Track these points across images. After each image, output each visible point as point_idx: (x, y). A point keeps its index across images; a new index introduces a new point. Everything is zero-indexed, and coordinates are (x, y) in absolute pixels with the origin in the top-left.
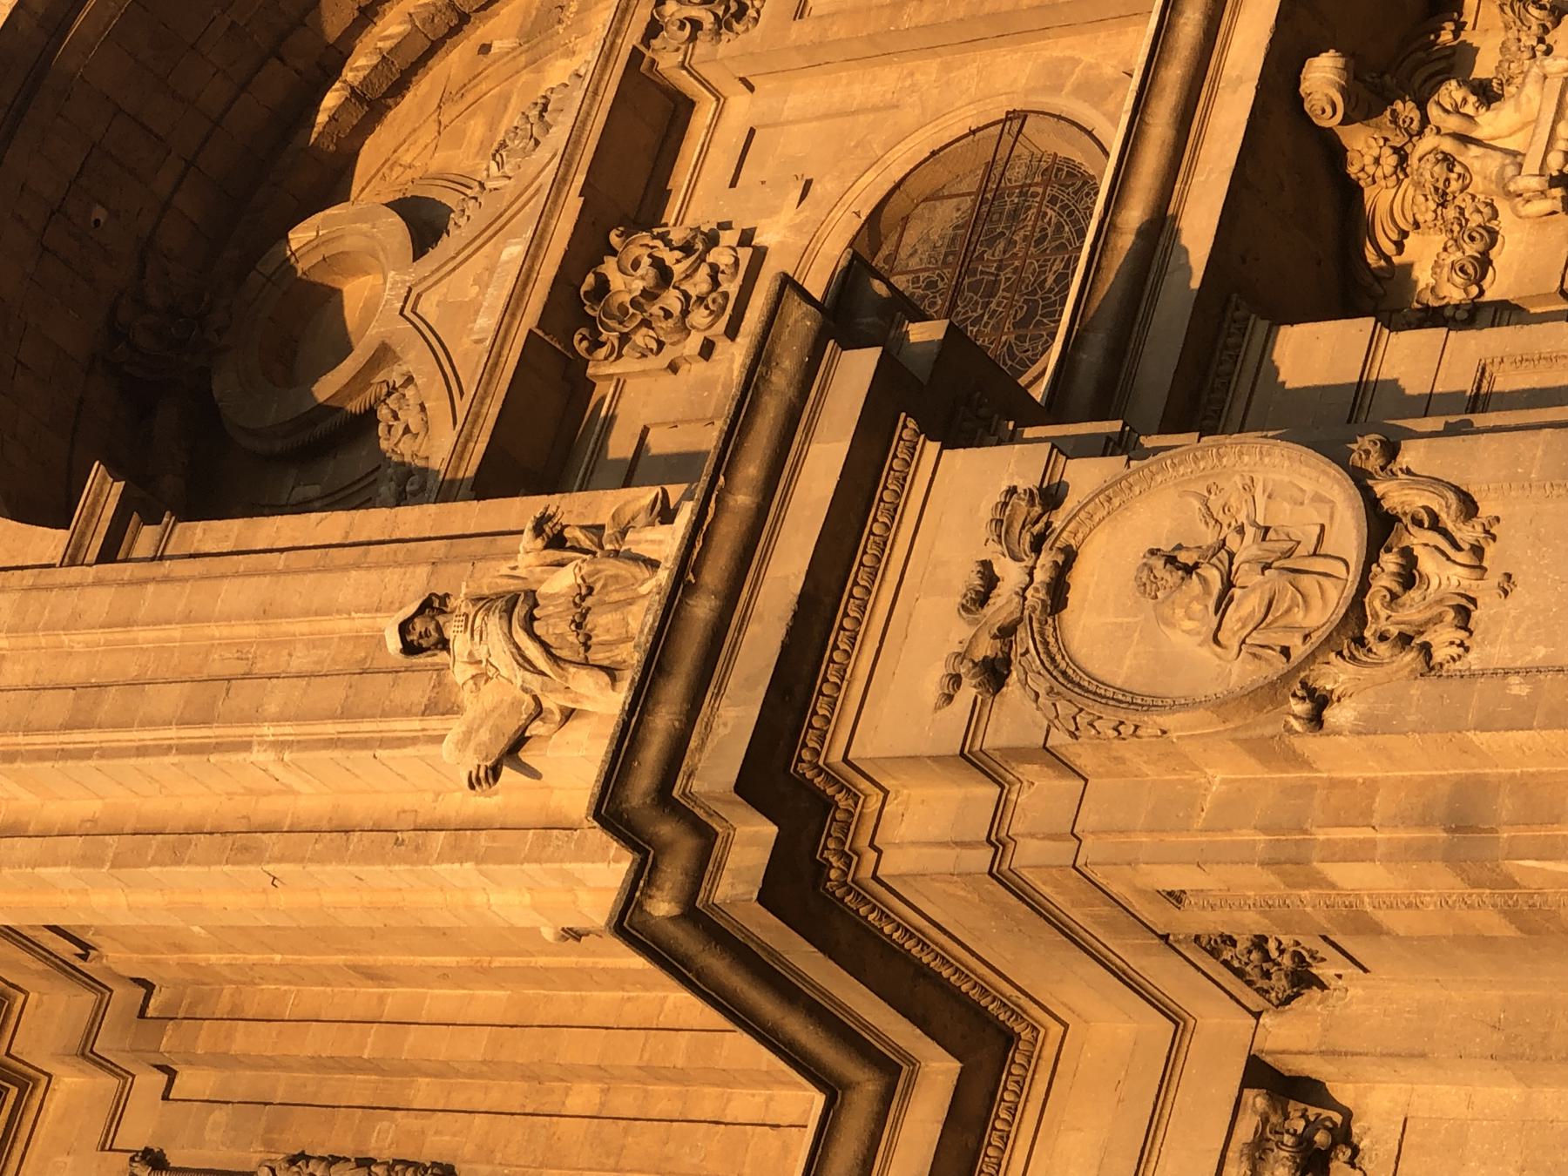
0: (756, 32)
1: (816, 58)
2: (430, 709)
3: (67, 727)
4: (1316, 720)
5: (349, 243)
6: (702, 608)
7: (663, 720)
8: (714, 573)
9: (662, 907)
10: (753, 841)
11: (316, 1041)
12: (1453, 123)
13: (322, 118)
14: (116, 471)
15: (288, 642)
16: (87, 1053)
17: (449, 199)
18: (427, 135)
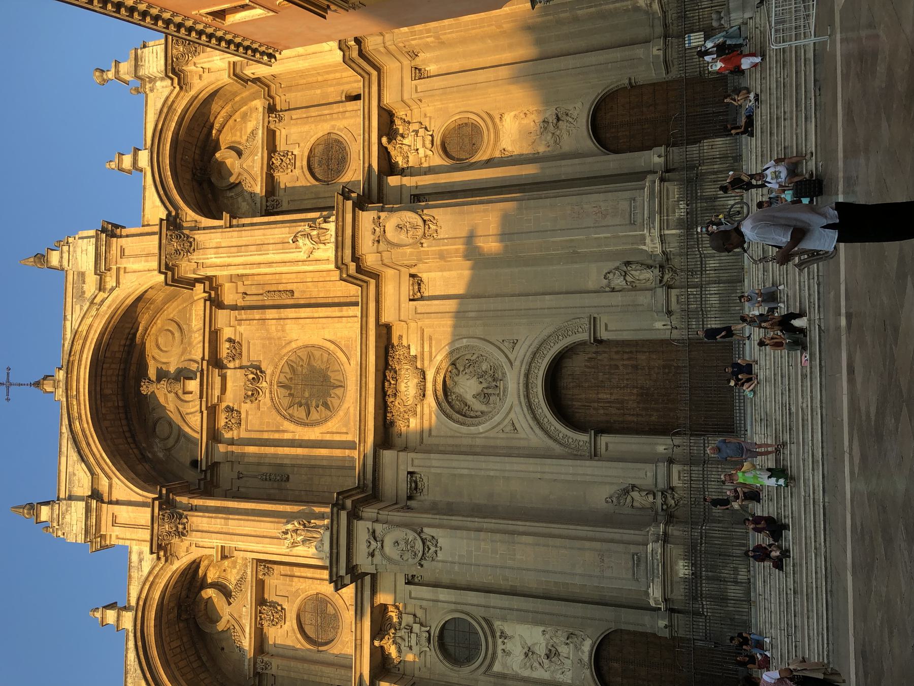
0: (285, 122)
1: (296, 124)
2: (296, 248)
3: (237, 253)
4: (422, 246)
5: (226, 156)
6: (340, 239)
7: (340, 254)
8: (340, 234)
9: (344, 276)
10: (353, 265)
11: (268, 277)
12: (400, 142)
13: (214, 135)
14: (227, 213)
15: (269, 239)
16: (231, 282)
17: (241, 147)
18: (230, 135)
